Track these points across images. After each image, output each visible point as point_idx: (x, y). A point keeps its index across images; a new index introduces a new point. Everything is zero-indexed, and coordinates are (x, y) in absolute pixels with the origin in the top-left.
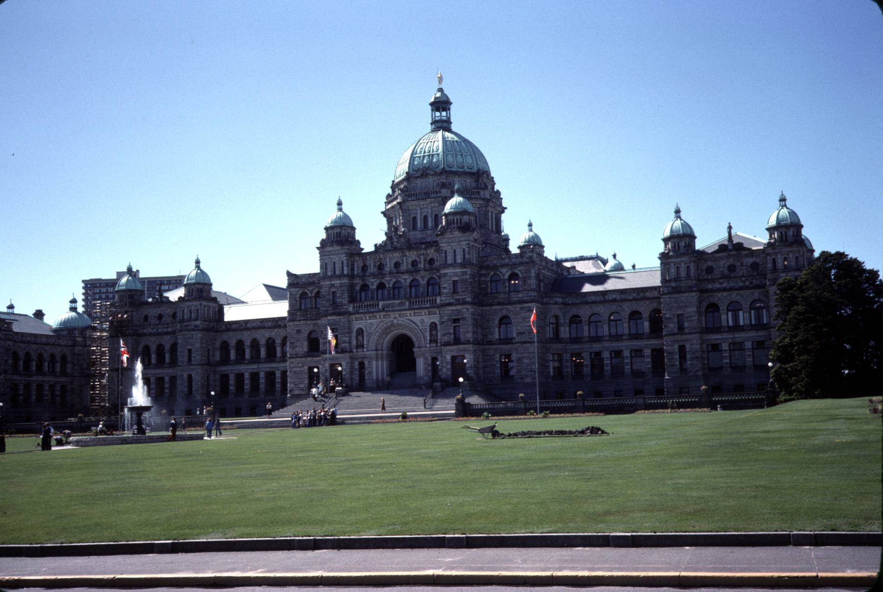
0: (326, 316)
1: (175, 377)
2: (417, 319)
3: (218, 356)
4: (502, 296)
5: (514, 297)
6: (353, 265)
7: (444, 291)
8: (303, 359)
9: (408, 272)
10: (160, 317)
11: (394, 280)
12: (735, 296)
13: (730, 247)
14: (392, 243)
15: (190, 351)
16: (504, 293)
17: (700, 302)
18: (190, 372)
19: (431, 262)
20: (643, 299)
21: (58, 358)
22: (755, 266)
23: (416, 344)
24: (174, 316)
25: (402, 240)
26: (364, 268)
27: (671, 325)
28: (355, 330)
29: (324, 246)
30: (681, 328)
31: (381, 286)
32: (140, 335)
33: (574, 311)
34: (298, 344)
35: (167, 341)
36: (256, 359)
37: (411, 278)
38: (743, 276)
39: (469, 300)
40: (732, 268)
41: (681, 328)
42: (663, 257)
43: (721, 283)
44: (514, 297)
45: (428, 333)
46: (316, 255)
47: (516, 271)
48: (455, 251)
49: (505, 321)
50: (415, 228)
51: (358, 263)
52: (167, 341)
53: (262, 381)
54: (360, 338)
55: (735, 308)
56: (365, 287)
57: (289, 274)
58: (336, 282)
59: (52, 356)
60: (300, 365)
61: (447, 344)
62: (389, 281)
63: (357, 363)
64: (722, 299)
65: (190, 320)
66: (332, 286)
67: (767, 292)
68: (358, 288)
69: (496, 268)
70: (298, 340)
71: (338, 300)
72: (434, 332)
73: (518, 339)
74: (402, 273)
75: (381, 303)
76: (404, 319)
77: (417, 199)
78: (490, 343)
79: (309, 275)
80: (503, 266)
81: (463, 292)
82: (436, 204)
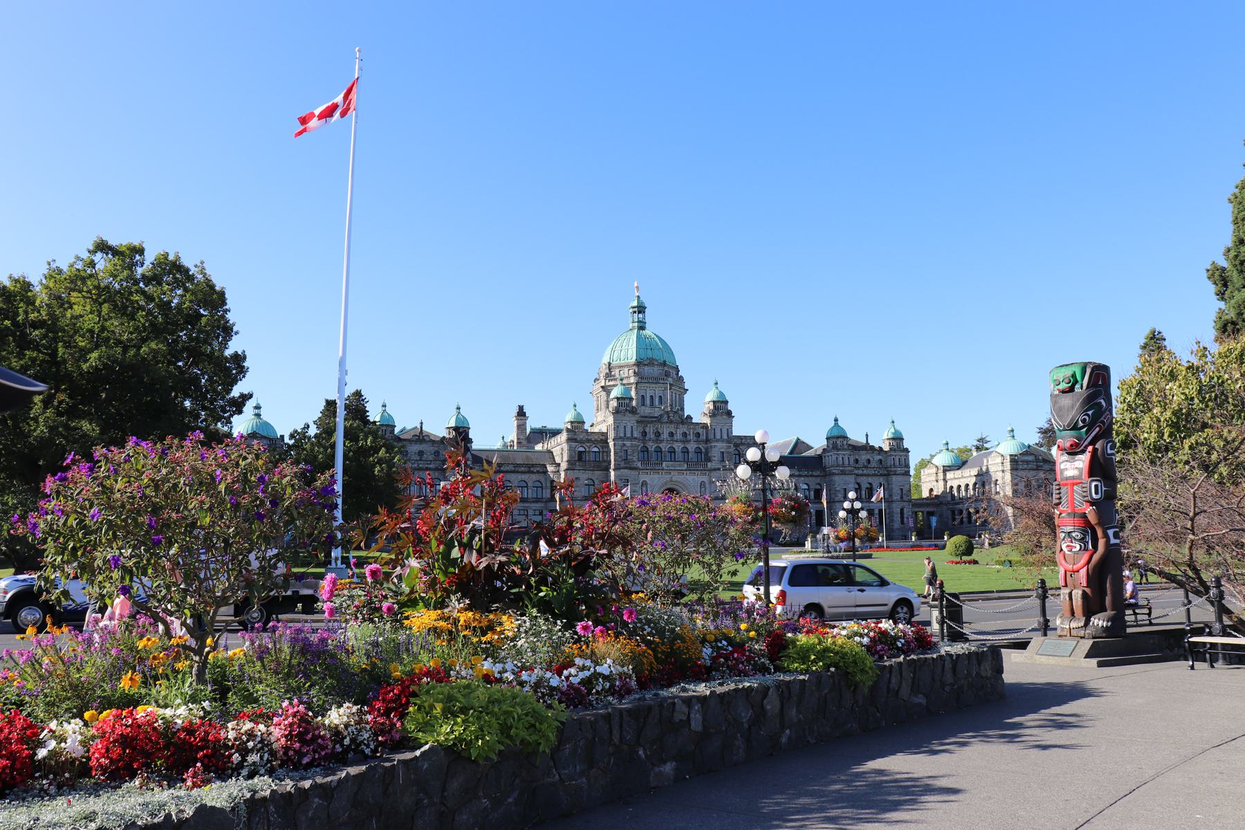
2: (690, 478)
10: (421, 453)
12: (870, 480)
19: (698, 435)
24: (437, 453)
25: (677, 417)
26: (644, 434)
56: (645, 450)
58: (628, 443)
62: (665, 447)
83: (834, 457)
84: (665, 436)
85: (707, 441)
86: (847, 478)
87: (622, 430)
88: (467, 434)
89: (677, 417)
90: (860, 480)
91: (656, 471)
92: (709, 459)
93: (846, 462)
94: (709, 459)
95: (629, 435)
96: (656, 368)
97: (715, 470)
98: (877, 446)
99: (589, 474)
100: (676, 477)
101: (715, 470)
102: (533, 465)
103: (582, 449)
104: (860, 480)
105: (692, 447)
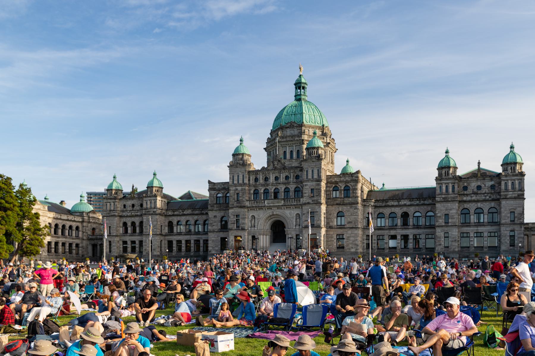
0: (232, 208)
1: (142, 241)
3: (166, 230)
4: (339, 200)
6: (249, 178)
7: (305, 195)
8: (218, 234)
9: (284, 183)
10: (133, 206)
11: (274, 188)
12: (479, 205)
13: (479, 175)
14: (274, 165)
16: (341, 198)
17: (459, 208)
21: (74, 228)
22: (492, 187)
23: (286, 227)
24: (142, 205)
25: (280, 165)
26: (256, 180)
27: (440, 221)
28: (250, 217)
29: (231, 166)
30: (447, 223)
31: (266, 192)
32: (121, 217)
33: (381, 210)
34: (215, 224)
35: (137, 220)
37: (285, 187)
38: (485, 193)
40: (479, 187)
41: (447, 223)
42: (437, 179)
43: (472, 197)
44: (347, 200)
45: (294, 220)
46: (227, 170)
47: (348, 185)
48: (313, 171)
50: (285, 158)
51: (252, 178)
52: (137, 220)
53: (192, 245)
54: (253, 222)
55: (479, 212)
56: (256, 193)
57: (210, 182)
58: (239, 188)
59: (71, 227)
60: (216, 236)
63: (250, 238)
64: (472, 207)
65: (151, 208)
66: (237, 189)
67: (500, 203)
68: (252, 192)
69: (336, 183)
70: (215, 222)
71: (240, 198)
72: (298, 220)
73: (348, 226)
74: (279, 184)
75: (266, 202)
77: (287, 141)
78: (331, 227)
79: (222, 183)
80: (341, 182)
81: (317, 196)
82: (299, 144)
84: (272, 179)
86: (449, 205)
87: (236, 178)
89: (280, 165)
91: (261, 208)
93: (450, 190)
94: (302, 197)
95: (241, 182)
96: (295, 130)
97: (305, 204)
99: (222, 214)
100: (277, 212)
101: (305, 204)
103: (219, 195)
104: (466, 206)
105: (292, 187)
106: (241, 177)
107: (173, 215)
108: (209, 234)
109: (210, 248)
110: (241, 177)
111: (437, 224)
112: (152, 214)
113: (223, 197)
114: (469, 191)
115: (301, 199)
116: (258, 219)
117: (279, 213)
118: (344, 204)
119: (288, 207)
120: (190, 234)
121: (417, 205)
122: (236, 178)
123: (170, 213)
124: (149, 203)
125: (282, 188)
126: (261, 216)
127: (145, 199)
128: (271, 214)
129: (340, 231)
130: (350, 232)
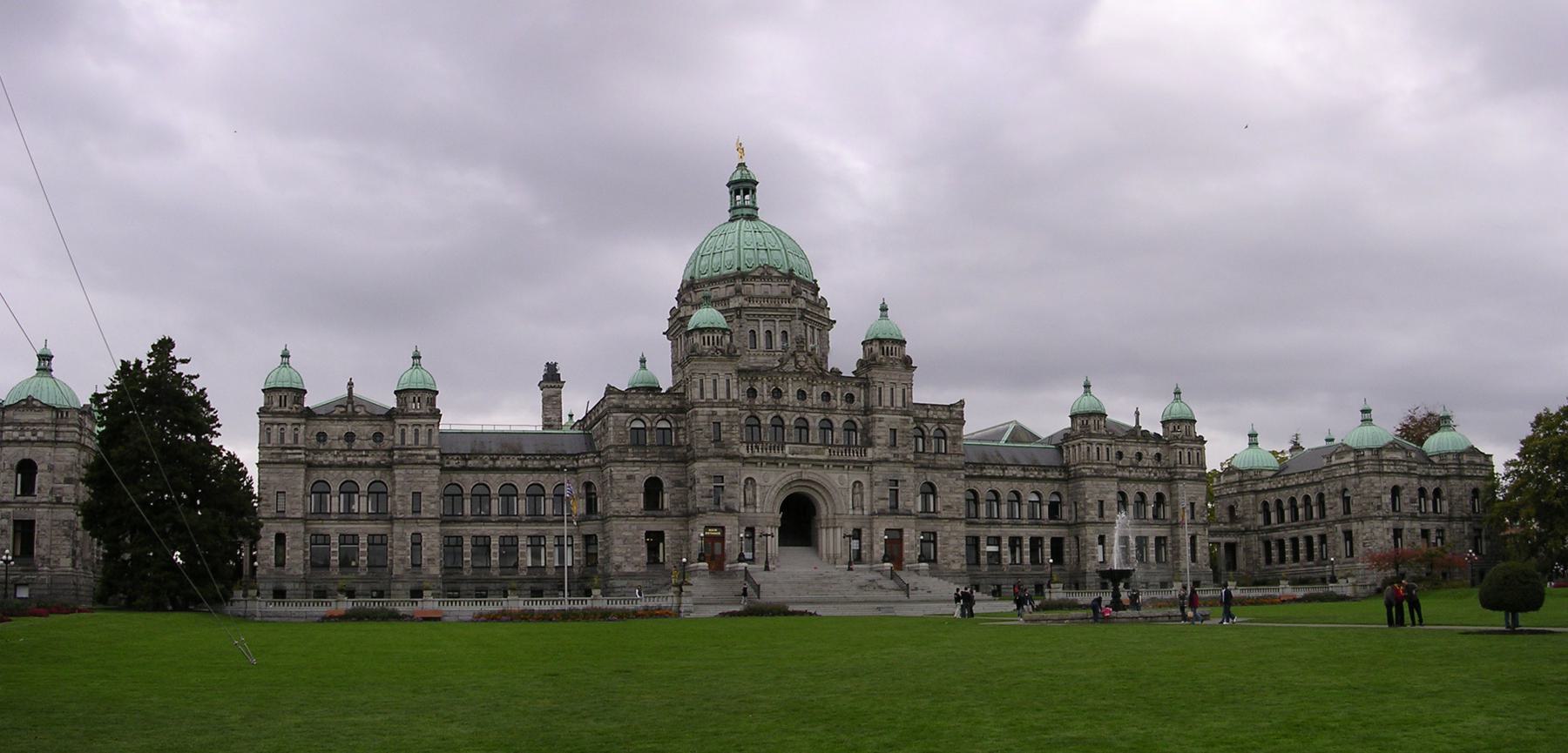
5: (942, 461)
10: (350, 437)
12: (1142, 487)
15: (417, 495)
18: (420, 530)
20: (1045, 479)
22: (1158, 456)
33: (973, 484)
36: (508, 517)
39: (911, 457)
40: (1139, 456)
41: (1101, 515)
44: (942, 461)
49: (929, 490)
52: (363, 479)
58: (721, 411)
61: (882, 513)
66: (714, 414)
73: (944, 514)
76: (819, 471)
83: (1084, 447)
85: (868, 410)
87: (708, 386)
88: (432, 402)
90: (1124, 487)
91: (774, 462)
92: (869, 443)
94: (869, 443)
95: (722, 395)
97: (879, 461)
98: (1152, 431)
102: (555, 456)
103: (639, 425)
104: (1124, 487)
105: (839, 421)
106: (722, 385)
107: (465, 469)
108: (615, 522)
109: (617, 559)
110: (722, 385)
111: (1087, 519)
112: (424, 463)
113: (651, 429)
114: (1125, 462)
115: (869, 451)
116: (763, 487)
117: (815, 478)
118: (938, 469)
119: (839, 465)
120: (518, 522)
121: (1036, 479)
122: (708, 386)
123: (453, 463)
124: (410, 432)
125: (815, 420)
126: (772, 481)
127: (399, 421)
128: (795, 477)
129: (929, 526)
130: (948, 528)
